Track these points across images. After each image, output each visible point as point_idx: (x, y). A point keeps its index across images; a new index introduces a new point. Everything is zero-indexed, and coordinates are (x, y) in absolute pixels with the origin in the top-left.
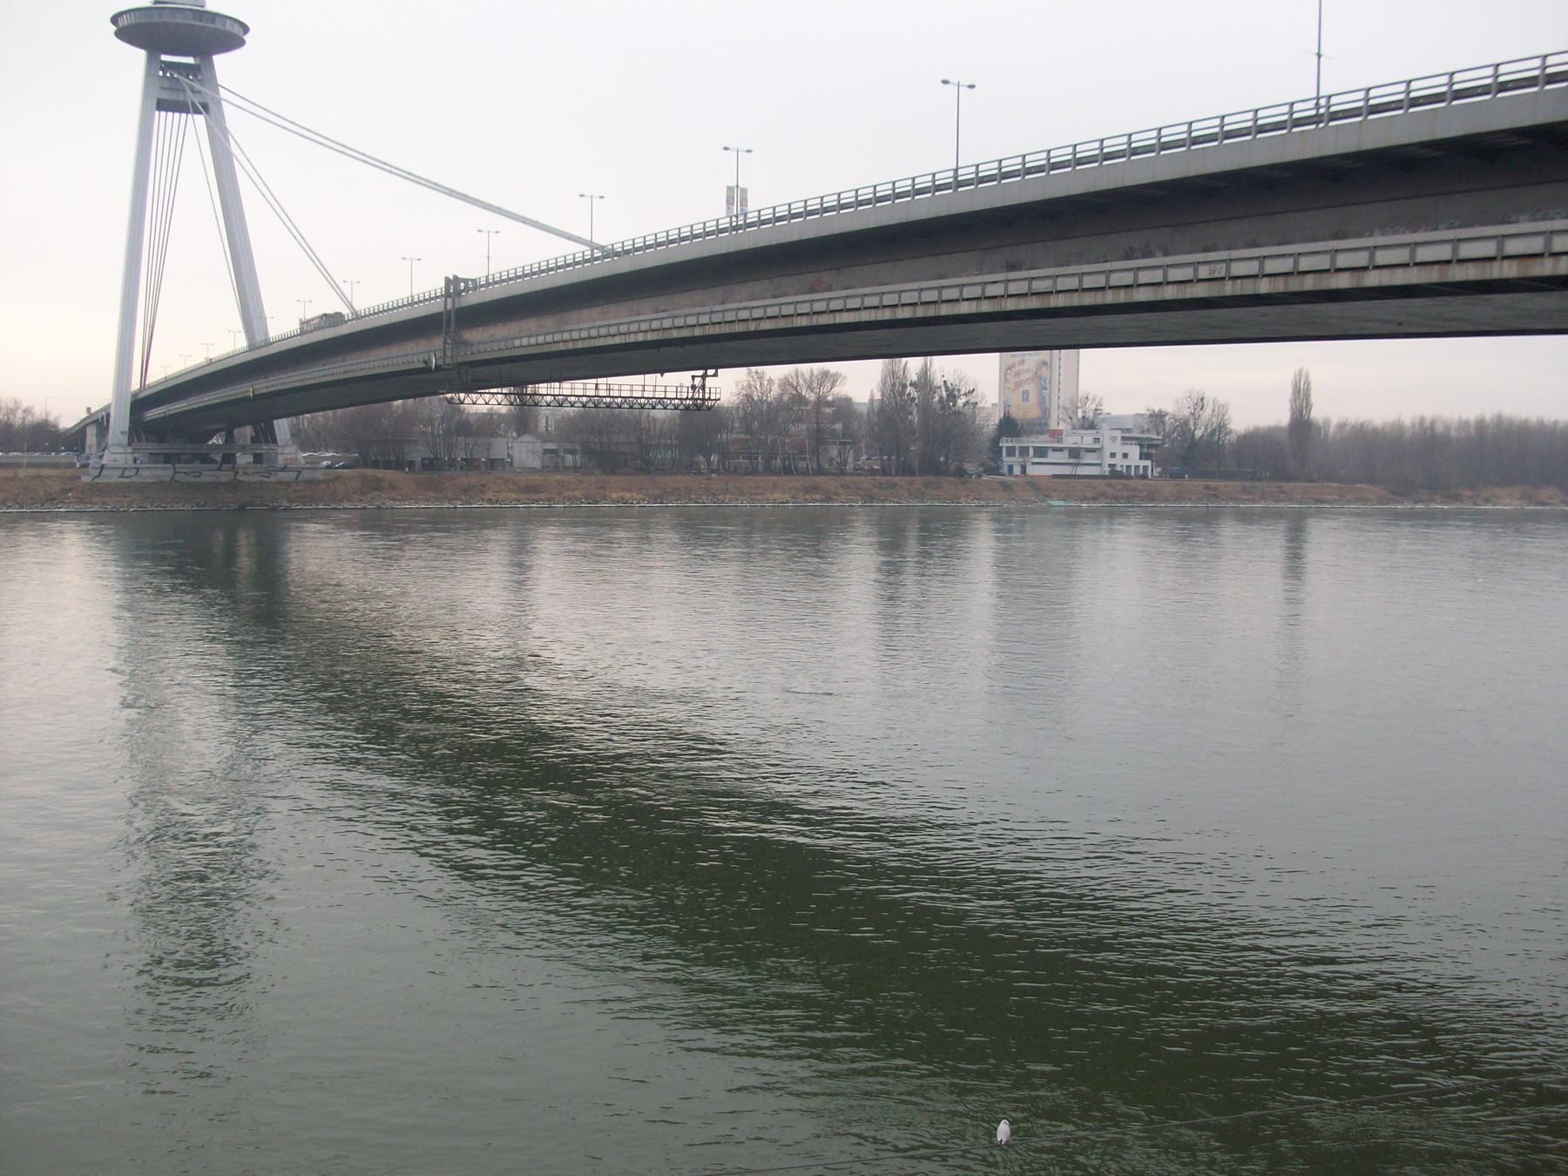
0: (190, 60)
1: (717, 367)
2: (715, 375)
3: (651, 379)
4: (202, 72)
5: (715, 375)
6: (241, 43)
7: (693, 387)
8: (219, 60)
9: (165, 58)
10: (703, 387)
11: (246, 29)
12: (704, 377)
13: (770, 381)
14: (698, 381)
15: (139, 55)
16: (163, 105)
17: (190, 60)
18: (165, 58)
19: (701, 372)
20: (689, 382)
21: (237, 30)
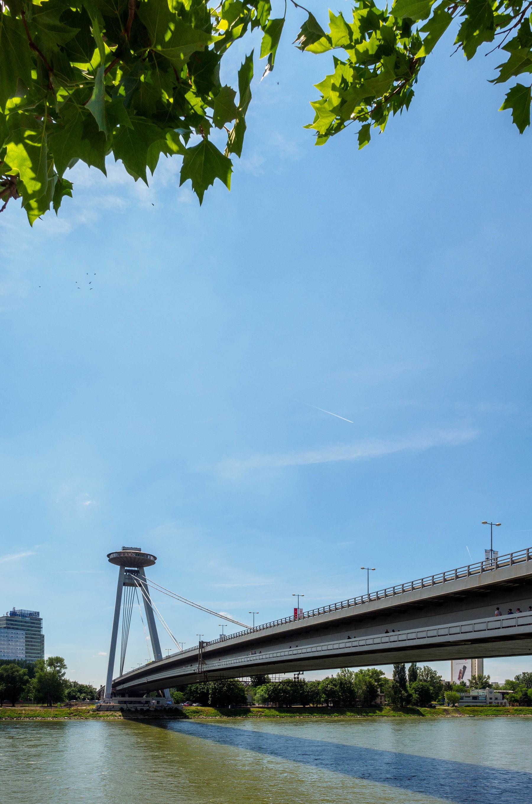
0: (136, 569)
1: (303, 671)
2: (303, 674)
3: (277, 675)
4: (139, 573)
5: (303, 674)
6: (153, 563)
7: (295, 678)
8: (146, 569)
9: (126, 568)
10: (298, 678)
11: (155, 558)
12: (298, 674)
13: (351, 674)
14: (296, 676)
15: (118, 567)
16: (124, 584)
17: (136, 569)
18: (126, 568)
19: (297, 673)
20: (293, 676)
21: (152, 558)
